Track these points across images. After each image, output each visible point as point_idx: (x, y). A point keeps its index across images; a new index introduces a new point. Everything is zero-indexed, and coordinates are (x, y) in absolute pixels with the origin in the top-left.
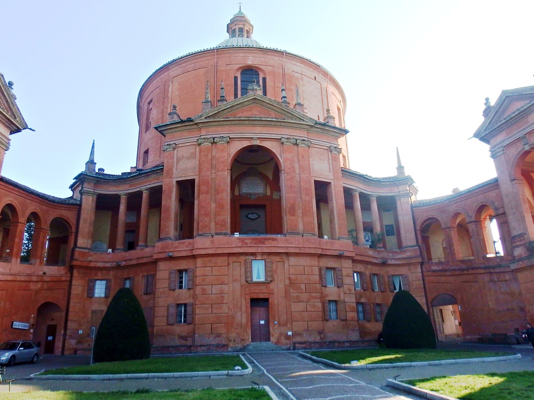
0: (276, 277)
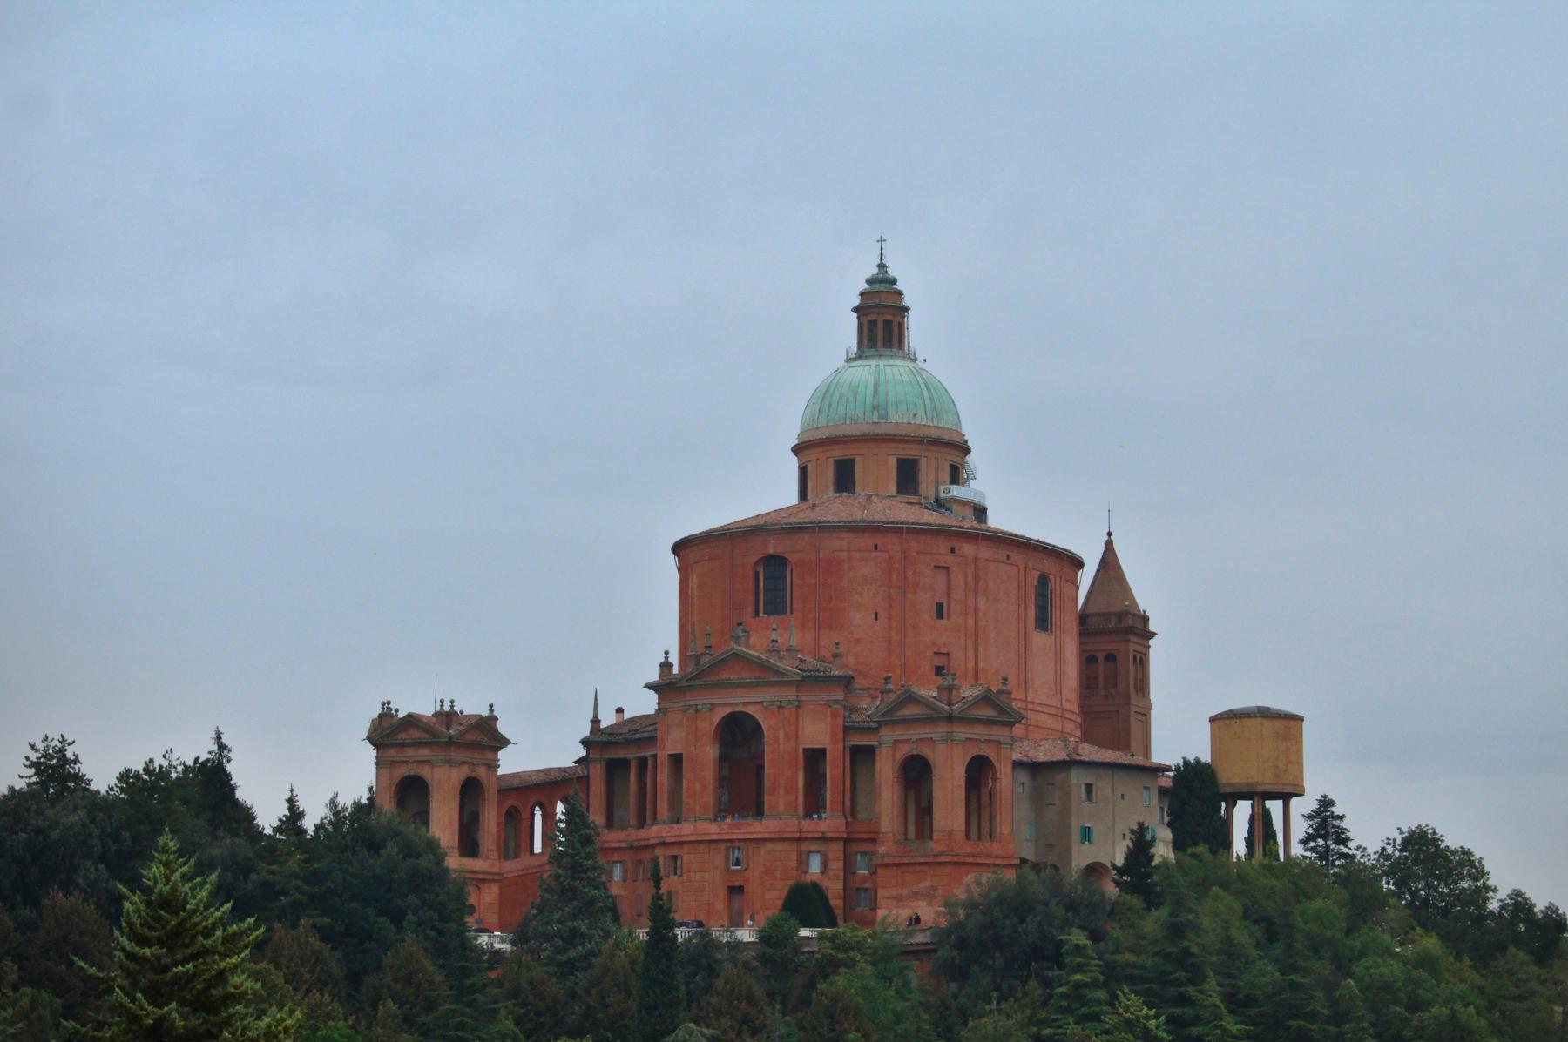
0: (751, 865)
